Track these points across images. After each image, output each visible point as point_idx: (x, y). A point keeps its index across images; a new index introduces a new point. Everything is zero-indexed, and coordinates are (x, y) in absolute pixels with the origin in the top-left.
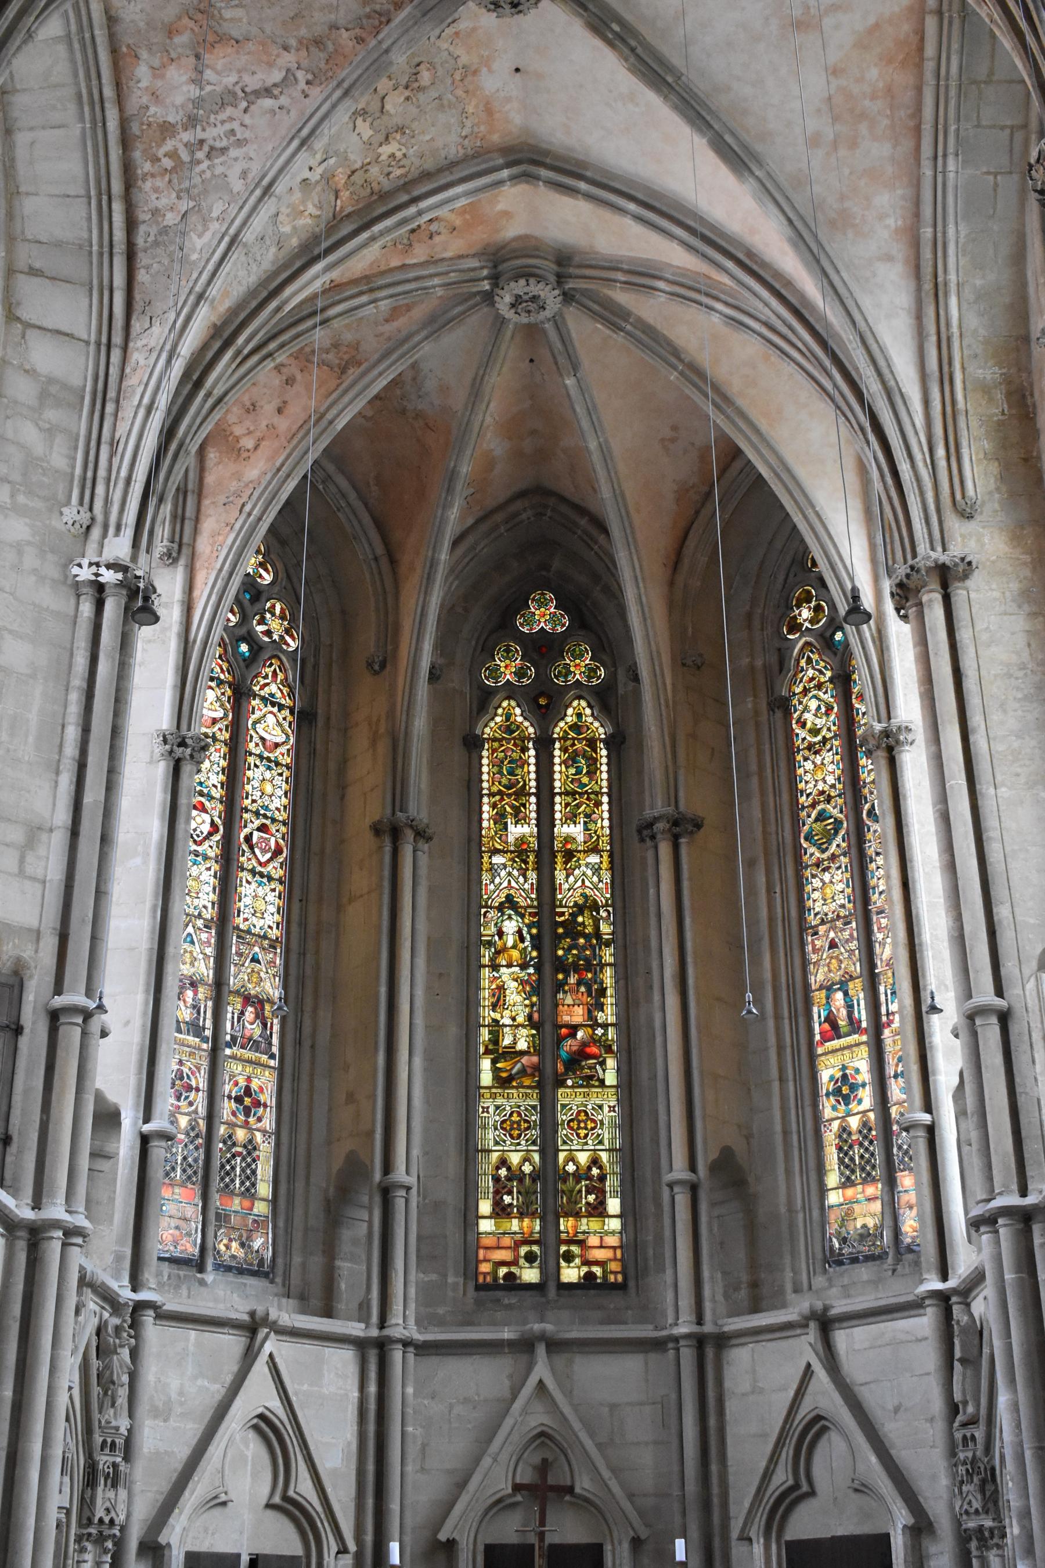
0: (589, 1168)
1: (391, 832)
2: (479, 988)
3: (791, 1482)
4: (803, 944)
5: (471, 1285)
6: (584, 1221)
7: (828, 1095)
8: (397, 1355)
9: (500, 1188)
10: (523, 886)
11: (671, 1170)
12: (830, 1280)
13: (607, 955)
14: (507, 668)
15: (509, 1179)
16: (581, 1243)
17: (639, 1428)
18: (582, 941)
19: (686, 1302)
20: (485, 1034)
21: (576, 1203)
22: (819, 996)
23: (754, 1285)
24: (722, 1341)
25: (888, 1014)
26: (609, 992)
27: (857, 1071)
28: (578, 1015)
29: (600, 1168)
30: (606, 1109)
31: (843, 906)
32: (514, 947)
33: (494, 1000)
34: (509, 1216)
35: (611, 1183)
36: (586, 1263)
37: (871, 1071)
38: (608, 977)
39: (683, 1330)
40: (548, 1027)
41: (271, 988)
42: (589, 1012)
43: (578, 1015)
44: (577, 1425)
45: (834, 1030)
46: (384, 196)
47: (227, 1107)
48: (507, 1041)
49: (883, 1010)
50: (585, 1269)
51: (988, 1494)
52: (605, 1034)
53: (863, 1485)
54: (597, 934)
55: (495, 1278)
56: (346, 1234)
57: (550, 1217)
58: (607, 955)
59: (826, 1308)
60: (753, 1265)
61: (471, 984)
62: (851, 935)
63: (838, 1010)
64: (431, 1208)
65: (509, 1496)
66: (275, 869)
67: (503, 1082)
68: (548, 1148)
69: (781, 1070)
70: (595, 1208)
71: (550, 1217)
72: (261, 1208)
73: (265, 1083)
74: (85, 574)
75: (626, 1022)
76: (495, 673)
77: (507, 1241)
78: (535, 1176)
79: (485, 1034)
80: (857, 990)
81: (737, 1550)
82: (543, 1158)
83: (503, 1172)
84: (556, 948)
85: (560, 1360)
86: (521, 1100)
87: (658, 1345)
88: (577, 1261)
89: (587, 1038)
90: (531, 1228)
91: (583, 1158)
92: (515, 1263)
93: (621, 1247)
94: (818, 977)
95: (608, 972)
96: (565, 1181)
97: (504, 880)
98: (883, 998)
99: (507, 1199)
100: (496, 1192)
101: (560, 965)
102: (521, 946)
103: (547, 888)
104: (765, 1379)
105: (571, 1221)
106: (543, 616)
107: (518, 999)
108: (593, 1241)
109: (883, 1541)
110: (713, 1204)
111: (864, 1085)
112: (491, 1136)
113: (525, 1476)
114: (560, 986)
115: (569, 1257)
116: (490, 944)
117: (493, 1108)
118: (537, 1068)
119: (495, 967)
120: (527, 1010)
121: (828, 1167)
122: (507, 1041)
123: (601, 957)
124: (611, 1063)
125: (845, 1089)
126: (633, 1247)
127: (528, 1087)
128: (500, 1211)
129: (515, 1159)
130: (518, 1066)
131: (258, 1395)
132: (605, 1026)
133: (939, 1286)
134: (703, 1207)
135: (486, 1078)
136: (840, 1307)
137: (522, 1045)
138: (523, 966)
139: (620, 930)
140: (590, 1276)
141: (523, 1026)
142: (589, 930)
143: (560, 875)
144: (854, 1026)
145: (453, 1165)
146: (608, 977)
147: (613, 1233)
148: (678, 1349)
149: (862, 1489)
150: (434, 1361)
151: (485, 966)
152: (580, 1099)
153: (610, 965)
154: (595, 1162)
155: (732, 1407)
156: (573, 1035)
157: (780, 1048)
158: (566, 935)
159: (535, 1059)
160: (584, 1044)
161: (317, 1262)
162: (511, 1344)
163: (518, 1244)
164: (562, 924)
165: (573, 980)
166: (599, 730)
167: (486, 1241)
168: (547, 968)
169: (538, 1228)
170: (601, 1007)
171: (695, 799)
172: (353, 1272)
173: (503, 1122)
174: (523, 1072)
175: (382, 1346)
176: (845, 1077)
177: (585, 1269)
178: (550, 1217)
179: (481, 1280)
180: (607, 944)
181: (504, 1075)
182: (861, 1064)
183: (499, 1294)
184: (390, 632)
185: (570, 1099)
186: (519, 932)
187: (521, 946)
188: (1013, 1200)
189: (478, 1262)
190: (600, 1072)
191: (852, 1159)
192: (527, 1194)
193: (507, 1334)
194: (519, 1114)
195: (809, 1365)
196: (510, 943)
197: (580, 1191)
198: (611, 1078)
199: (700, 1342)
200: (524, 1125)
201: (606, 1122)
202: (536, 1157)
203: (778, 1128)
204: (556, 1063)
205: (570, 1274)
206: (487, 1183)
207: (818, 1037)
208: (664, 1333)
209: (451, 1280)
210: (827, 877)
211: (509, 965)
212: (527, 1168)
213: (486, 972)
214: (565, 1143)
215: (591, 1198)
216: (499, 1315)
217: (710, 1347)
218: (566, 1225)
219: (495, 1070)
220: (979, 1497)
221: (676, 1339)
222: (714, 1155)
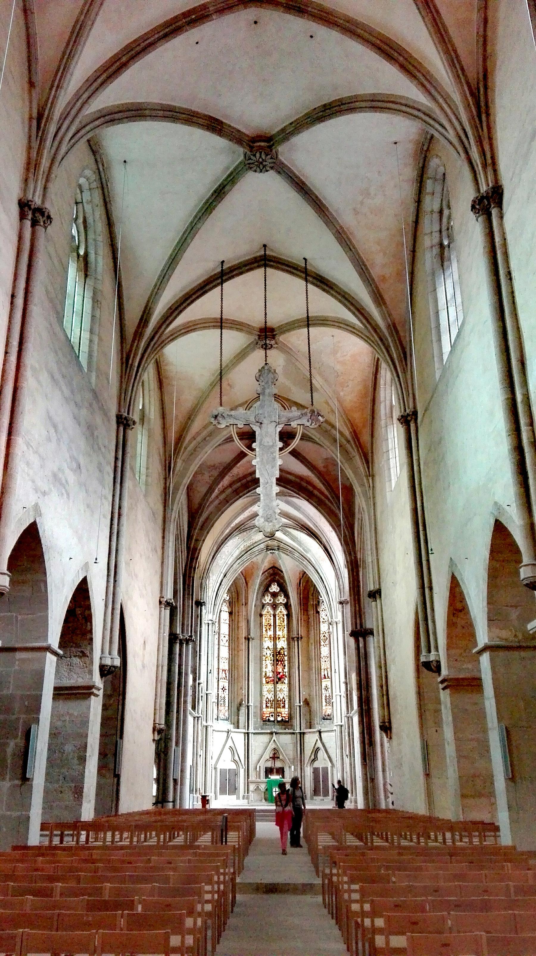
1: (248, 639)
8: (250, 735)
10: (270, 644)
14: (268, 599)
17: (291, 747)
19: (298, 727)
20: (264, 674)
22: (323, 671)
24: (304, 733)
38: (286, 663)
39: (298, 731)
41: (227, 668)
43: (280, 670)
46: (249, 547)
47: (220, 690)
56: (240, 712)
58: (286, 658)
61: (261, 664)
64: (255, 707)
66: (227, 644)
72: (227, 708)
73: (226, 685)
74: (206, 622)
76: (265, 600)
80: (329, 670)
81: (306, 768)
86: (271, 686)
87: (293, 733)
91: (281, 698)
94: (322, 668)
97: (268, 643)
101: (277, 660)
103: (275, 645)
104: (311, 740)
106: (274, 588)
113: (271, 756)
114: (277, 664)
118: (273, 680)
124: (286, 679)
125: (326, 689)
128: (267, 707)
129: (269, 698)
131: (230, 743)
135: (264, 682)
143: (277, 642)
144: (328, 678)
145: (259, 698)
146: (286, 663)
149: (325, 760)
150: (256, 736)
161: (236, 717)
166: (285, 612)
171: (302, 632)
172: (242, 719)
175: (248, 733)
178: (276, 708)
182: (329, 684)
184: (247, 599)
185: (279, 686)
192: (272, 704)
193: (269, 731)
199: (300, 733)
205: (279, 719)
206: (264, 702)
213: (264, 662)
217: (302, 734)
218: (278, 710)
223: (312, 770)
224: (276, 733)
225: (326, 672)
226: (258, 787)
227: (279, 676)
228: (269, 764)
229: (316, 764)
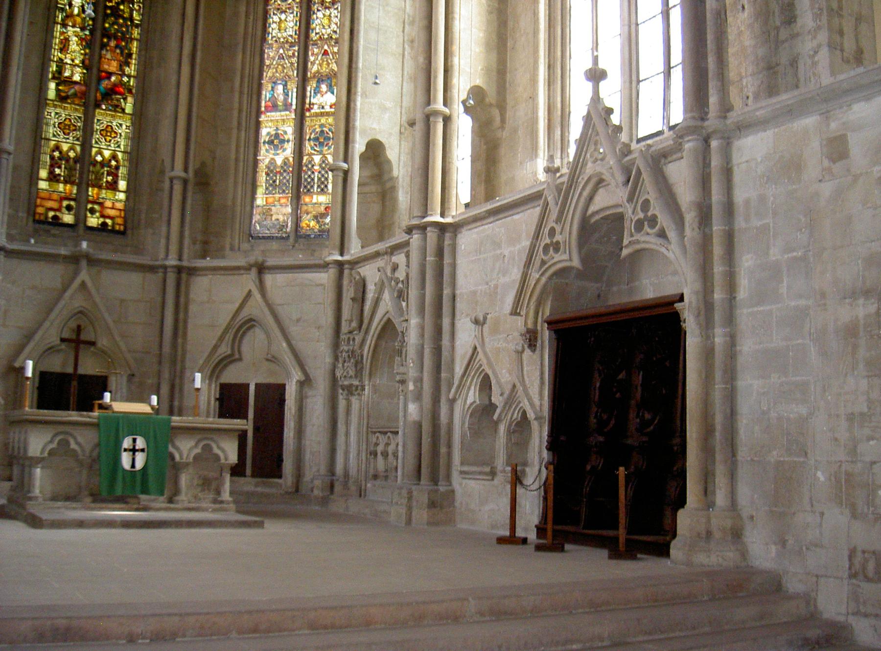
0: (110, 161)
2: (53, 37)
3: (229, 352)
4: (262, 52)
5: (31, 219)
6: (104, 191)
7: (264, 142)
9: (54, 164)
11: (173, 169)
12: (252, 246)
13: (136, 33)
15: (60, 159)
16: (101, 204)
18: (121, 21)
19: (174, 248)
20: (54, 67)
21: (101, 179)
23: (206, 243)
24: (192, 271)
25: (310, 104)
26: (134, 56)
27: (285, 133)
28: (113, 67)
29: (117, 161)
30: (124, 127)
31: (291, 36)
32: (78, 15)
33: (61, 46)
34: (58, 181)
35: (122, 171)
36: (103, 216)
37: (294, 133)
39: (172, 262)
40: (95, 71)
42: (121, 66)
43: (113, 67)
44: (103, 309)
45: (274, 107)
48: (67, 74)
49: (308, 101)
50: (102, 220)
51: (358, 368)
52: (129, 82)
53: (273, 357)
54: (131, 19)
55: (47, 217)
57: (83, 185)
58: (136, 33)
59: (264, 262)
60: (205, 232)
62: (293, 54)
63: (278, 95)
65: (58, 345)
67: (62, 98)
68: (86, 145)
69: (239, 124)
70: (111, 185)
71: (84, 186)
75: (141, 76)
77: (55, 196)
78: (76, 160)
79: (54, 67)
82: (83, 150)
83: (57, 154)
84: (104, 22)
85: (95, 270)
86: (72, 112)
87: (152, 269)
88: (98, 214)
89: (118, 81)
90: (71, 191)
91: (107, 154)
92: (59, 210)
93: (124, 210)
95: (135, 44)
96: (94, 165)
98: (308, 94)
99: (57, 171)
100: (52, 166)
101: (106, 33)
102: (83, 16)
105: (96, 190)
107: (77, 48)
108: (108, 204)
109: (282, 388)
110: (194, 193)
111: (288, 141)
112: (51, 131)
113: (66, 335)
114: (103, 46)
115: (92, 211)
116: (62, 10)
117: (54, 115)
118: (84, 95)
119: (64, 25)
120: (82, 57)
121: (259, 184)
122: (67, 74)
123: (132, 34)
126: (130, 210)
127: (78, 105)
128: (53, 178)
129: (65, 147)
130: (72, 91)
132: (129, 76)
133: (340, 258)
134: (190, 194)
135: (52, 94)
136: (270, 262)
137: (77, 78)
138: (83, 29)
139: (146, 18)
140: (104, 224)
141: (79, 66)
142: (126, 15)
144: (287, 107)
147: (121, 201)
148: (165, 273)
149: (273, 359)
150: (15, 262)
151: (58, 23)
152: (108, 119)
153: (137, 40)
154: (114, 157)
155: (193, 308)
156: (109, 78)
157: (240, 111)
158: (112, 15)
159: (83, 88)
160: (115, 85)
162: (65, 257)
163: (62, 199)
164: (111, 8)
165: (113, 43)
167: (42, 195)
168: (98, 34)
169: (75, 191)
170: (128, 64)
173: (60, 123)
174: (75, 95)
176: (277, 136)
177: (102, 220)
178: (83, 185)
179: (37, 217)
180: (137, 26)
181: (63, 94)
182: (289, 130)
183: (46, 227)
185: (102, 118)
186: (83, 6)
187: (83, 16)
188: (437, 218)
189: (36, 206)
190: (123, 104)
191: (274, 181)
192: (70, 169)
193: (63, 251)
194: (70, 120)
195: (250, 291)
196: (76, 11)
197: (103, 174)
198: (129, 108)
199: (179, 270)
200: (72, 128)
201: (123, 134)
202: (78, 148)
203: (233, 156)
204: (96, 93)
205: (93, 221)
207: (263, 109)
208: (157, 263)
209: (20, 214)
210: (283, 17)
211: (74, 26)
212: (72, 154)
214: (96, 143)
215: (110, 178)
216: (50, 240)
219: (57, 90)
220: (354, 369)
221: (165, 268)
222: (198, 165)
223: (215, 392)
224: (92, 262)
225: (280, 88)
226: (64, 443)
227: (105, 84)
228: (57, 364)
229: (232, 376)
